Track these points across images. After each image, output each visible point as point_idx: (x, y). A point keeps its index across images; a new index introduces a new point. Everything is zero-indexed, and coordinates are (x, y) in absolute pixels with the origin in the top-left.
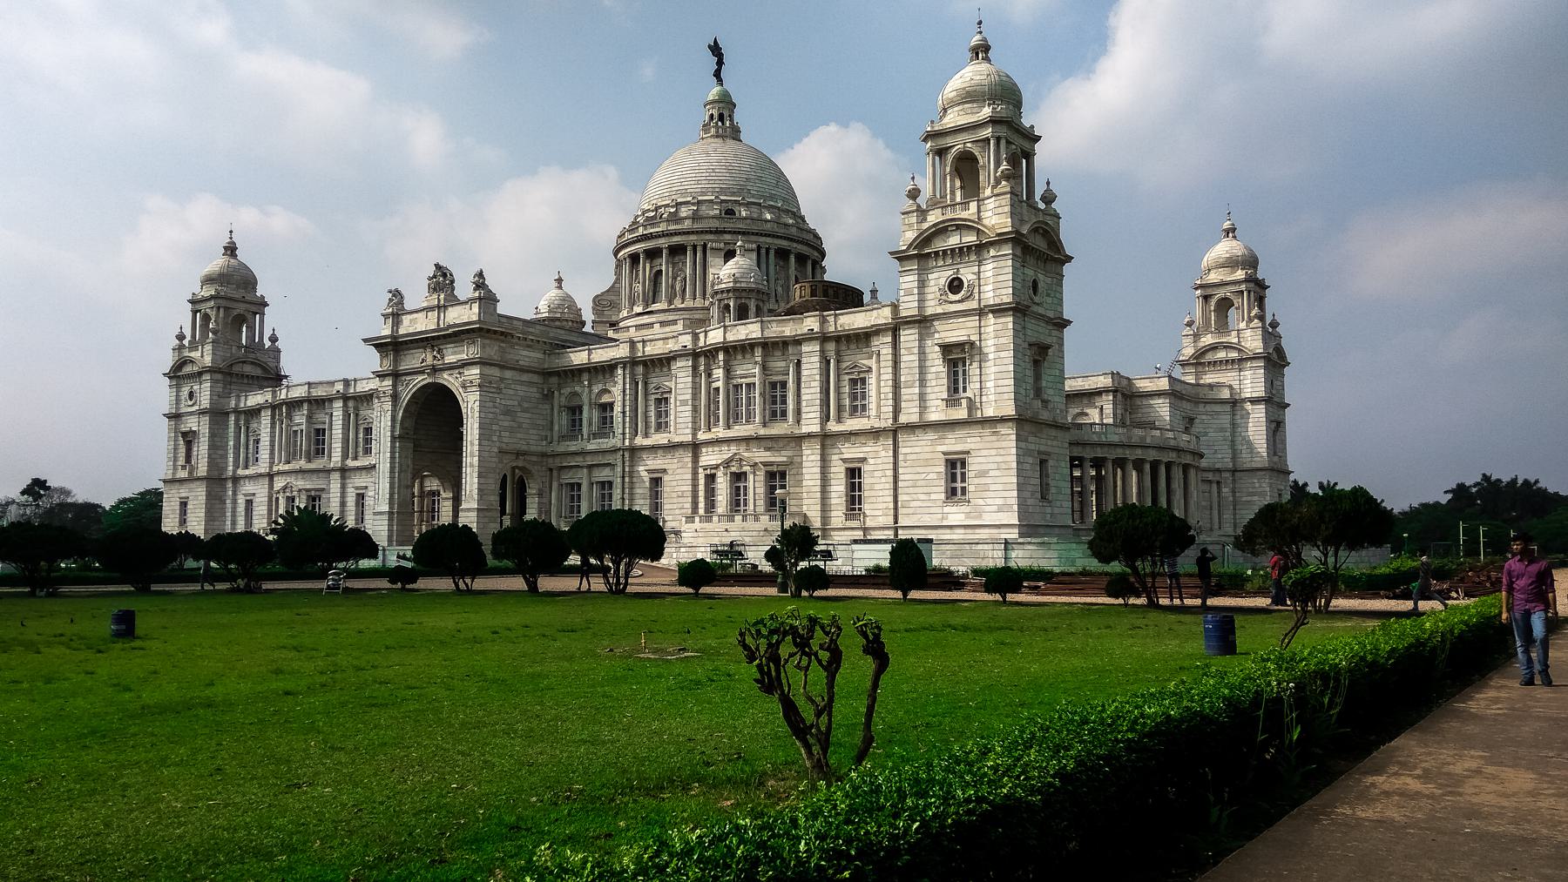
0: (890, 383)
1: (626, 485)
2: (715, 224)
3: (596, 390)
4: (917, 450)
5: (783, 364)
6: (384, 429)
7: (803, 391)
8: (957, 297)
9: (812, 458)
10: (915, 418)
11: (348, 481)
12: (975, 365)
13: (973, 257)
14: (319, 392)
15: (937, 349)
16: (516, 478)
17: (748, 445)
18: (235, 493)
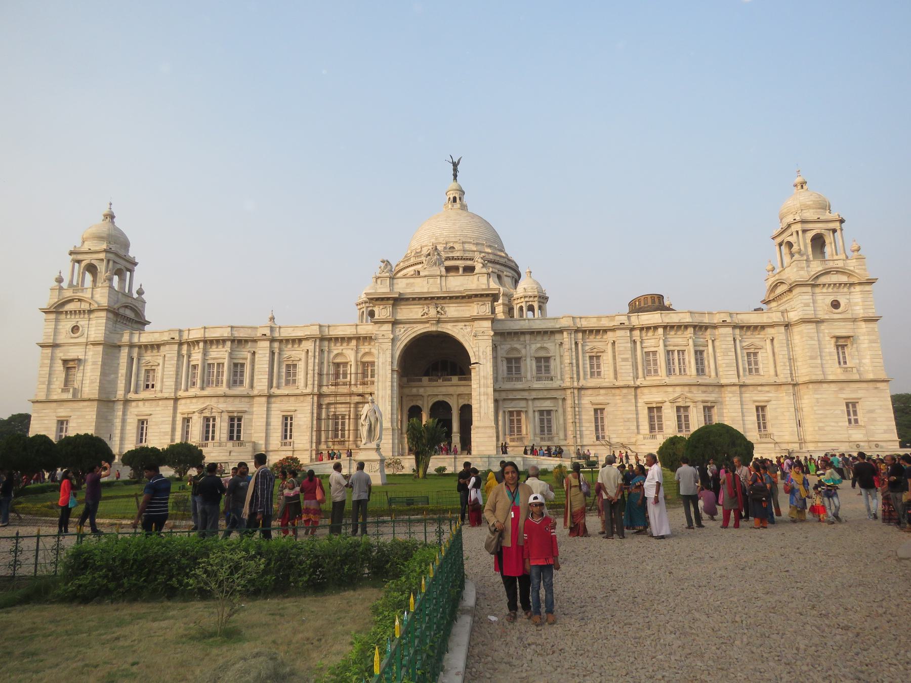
0: (787, 356)
1: (577, 413)
3: (534, 347)
4: (825, 396)
5: (702, 340)
6: (383, 363)
7: (719, 358)
8: (839, 310)
9: (733, 399)
10: (821, 378)
11: (273, 405)
12: (854, 350)
13: (846, 290)
15: (828, 338)
16: (460, 406)
18: (124, 414)
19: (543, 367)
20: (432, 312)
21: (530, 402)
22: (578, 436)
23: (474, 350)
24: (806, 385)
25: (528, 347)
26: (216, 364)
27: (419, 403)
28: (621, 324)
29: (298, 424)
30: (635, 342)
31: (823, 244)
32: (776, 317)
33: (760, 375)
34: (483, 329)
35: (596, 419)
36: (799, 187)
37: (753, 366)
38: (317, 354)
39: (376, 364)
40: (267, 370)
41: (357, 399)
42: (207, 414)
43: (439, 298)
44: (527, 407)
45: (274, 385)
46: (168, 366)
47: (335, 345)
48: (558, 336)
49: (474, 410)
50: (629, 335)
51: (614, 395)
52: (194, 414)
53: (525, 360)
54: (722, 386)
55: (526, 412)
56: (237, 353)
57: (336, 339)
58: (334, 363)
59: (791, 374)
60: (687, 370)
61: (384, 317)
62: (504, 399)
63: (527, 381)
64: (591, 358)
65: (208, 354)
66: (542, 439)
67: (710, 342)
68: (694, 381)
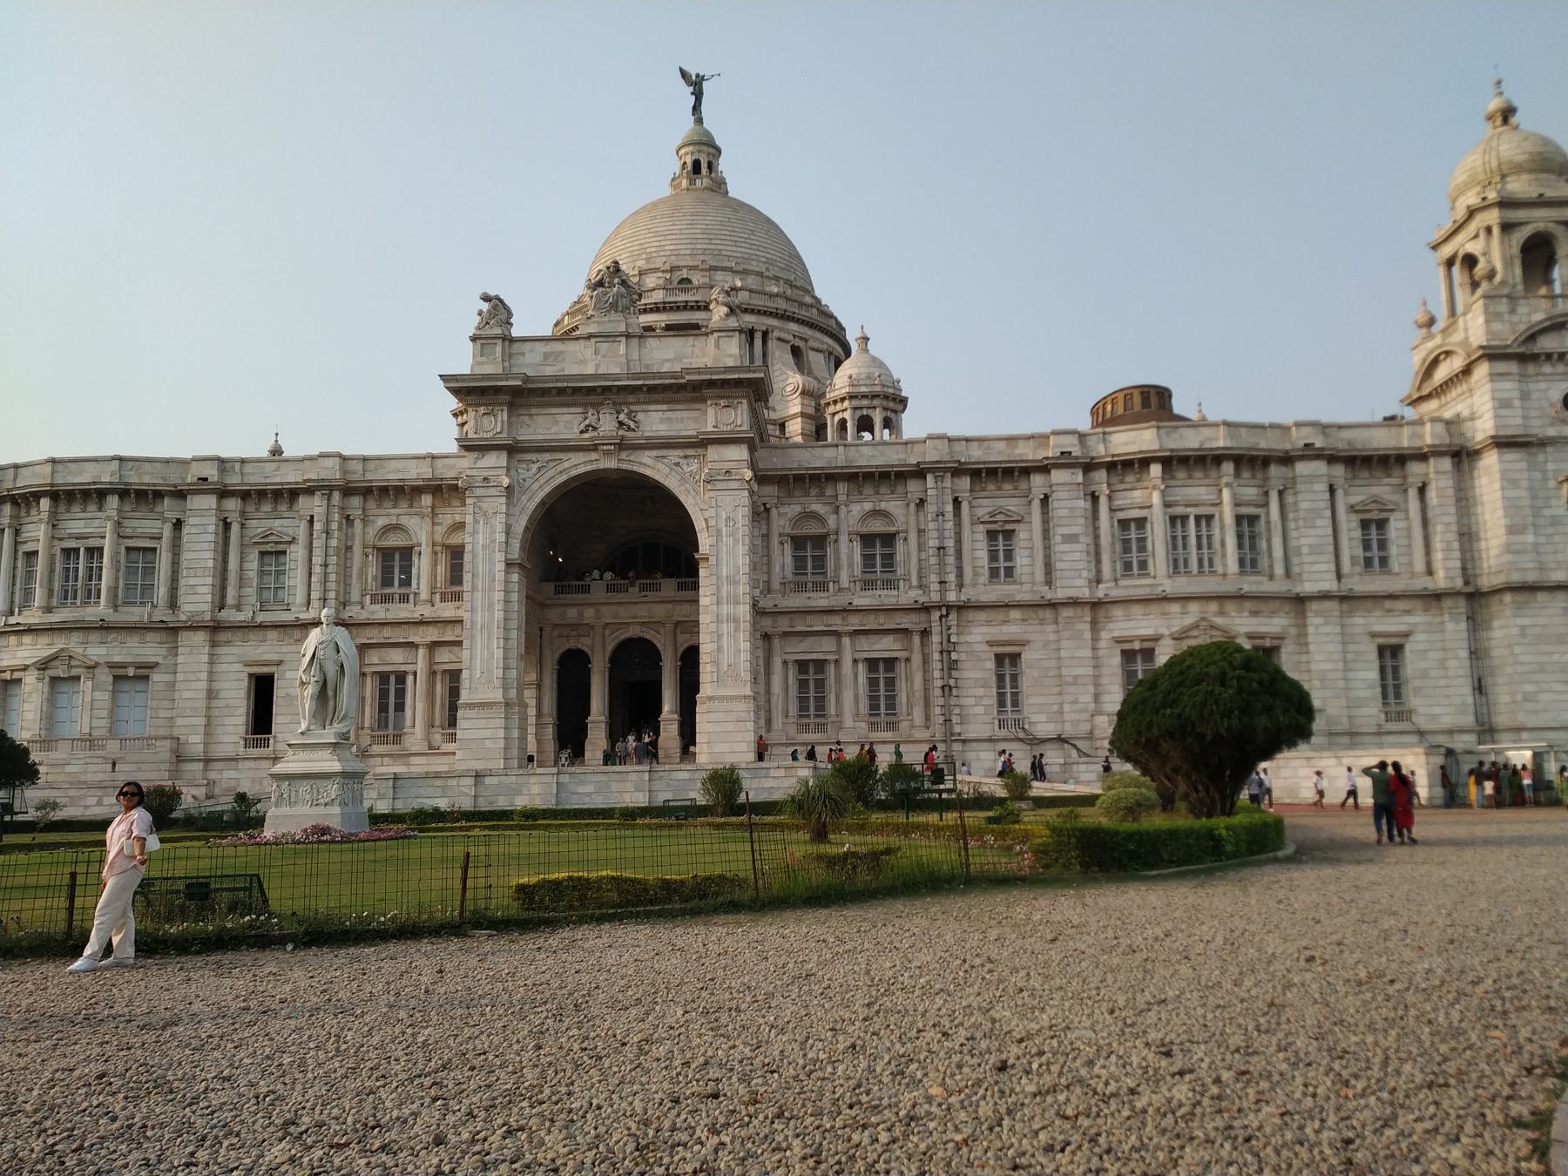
0: (1454, 528)
2: (781, 304)
4: (1541, 621)
9: (1327, 629)
10: (1531, 577)
14: (146, 478)
16: (681, 650)
17: (1221, 606)
19: (878, 558)
20: (607, 424)
21: (846, 641)
22: (955, 719)
23: (707, 514)
25: (843, 510)
27: (584, 644)
28: (1062, 453)
30: (1095, 498)
31: (1550, 262)
32: (1429, 436)
33: (1390, 573)
34: (726, 466)
35: (1000, 679)
36: (1499, 121)
37: (1375, 552)
38: (334, 526)
39: (468, 548)
40: (211, 564)
41: (432, 634)
43: (621, 389)
44: (839, 651)
45: (230, 600)
47: (379, 507)
48: (913, 486)
49: (704, 658)
50: (1080, 478)
51: (1042, 622)
53: (836, 541)
55: (837, 662)
56: (134, 523)
57: (384, 491)
58: (379, 549)
59: (1464, 569)
61: (489, 435)
62: (786, 634)
63: (840, 590)
64: (992, 535)
65: (62, 525)
66: (873, 726)
67: (1274, 496)
68: (1229, 587)
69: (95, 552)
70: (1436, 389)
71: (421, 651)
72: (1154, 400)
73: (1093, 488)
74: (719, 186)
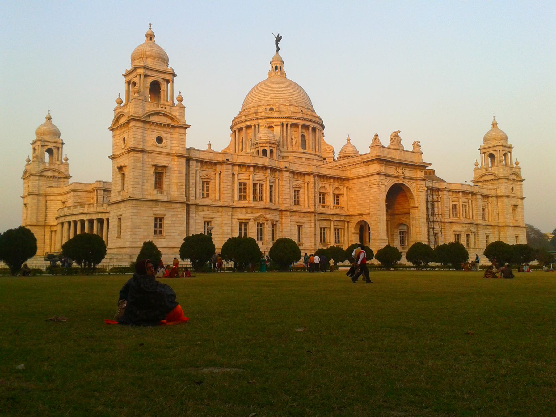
9: (481, 232)
15: (510, 205)
20: (401, 172)
24: (503, 227)
26: (259, 184)
29: (306, 232)
32: (493, 193)
33: (485, 220)
34: (422, 186)
40: (289, 192)
41: (335, 218)
42: (261, 221)
43: (405, 164)
46: (227, 182)
52: (250, 221)
54: (477, 225)
55: (408, 233)
60: (468, 216)
61: (382, 171)
69: (261, 185)
70: (484, 181)
71: (332, 222)
72: (432, 173)
73: (449, 196)
74: (283, 74)
